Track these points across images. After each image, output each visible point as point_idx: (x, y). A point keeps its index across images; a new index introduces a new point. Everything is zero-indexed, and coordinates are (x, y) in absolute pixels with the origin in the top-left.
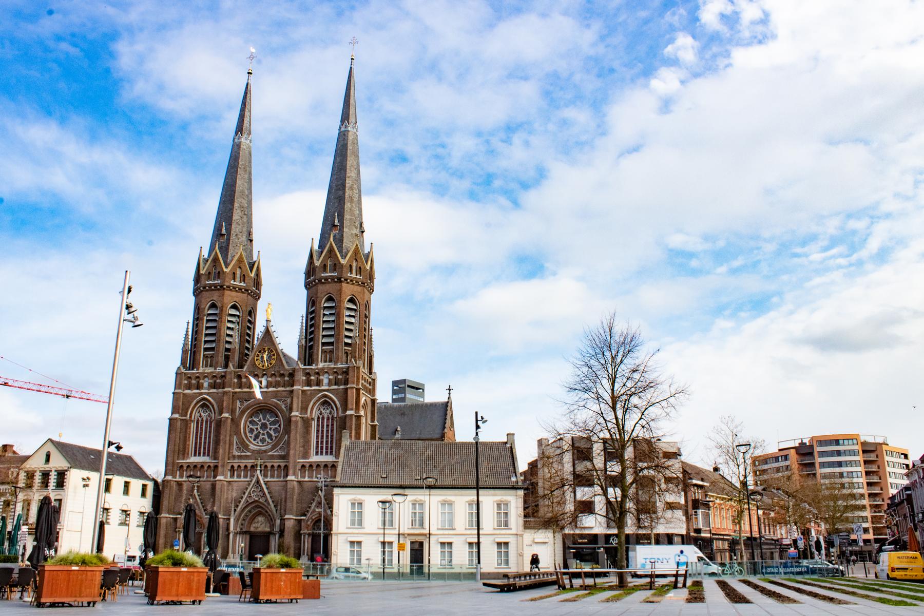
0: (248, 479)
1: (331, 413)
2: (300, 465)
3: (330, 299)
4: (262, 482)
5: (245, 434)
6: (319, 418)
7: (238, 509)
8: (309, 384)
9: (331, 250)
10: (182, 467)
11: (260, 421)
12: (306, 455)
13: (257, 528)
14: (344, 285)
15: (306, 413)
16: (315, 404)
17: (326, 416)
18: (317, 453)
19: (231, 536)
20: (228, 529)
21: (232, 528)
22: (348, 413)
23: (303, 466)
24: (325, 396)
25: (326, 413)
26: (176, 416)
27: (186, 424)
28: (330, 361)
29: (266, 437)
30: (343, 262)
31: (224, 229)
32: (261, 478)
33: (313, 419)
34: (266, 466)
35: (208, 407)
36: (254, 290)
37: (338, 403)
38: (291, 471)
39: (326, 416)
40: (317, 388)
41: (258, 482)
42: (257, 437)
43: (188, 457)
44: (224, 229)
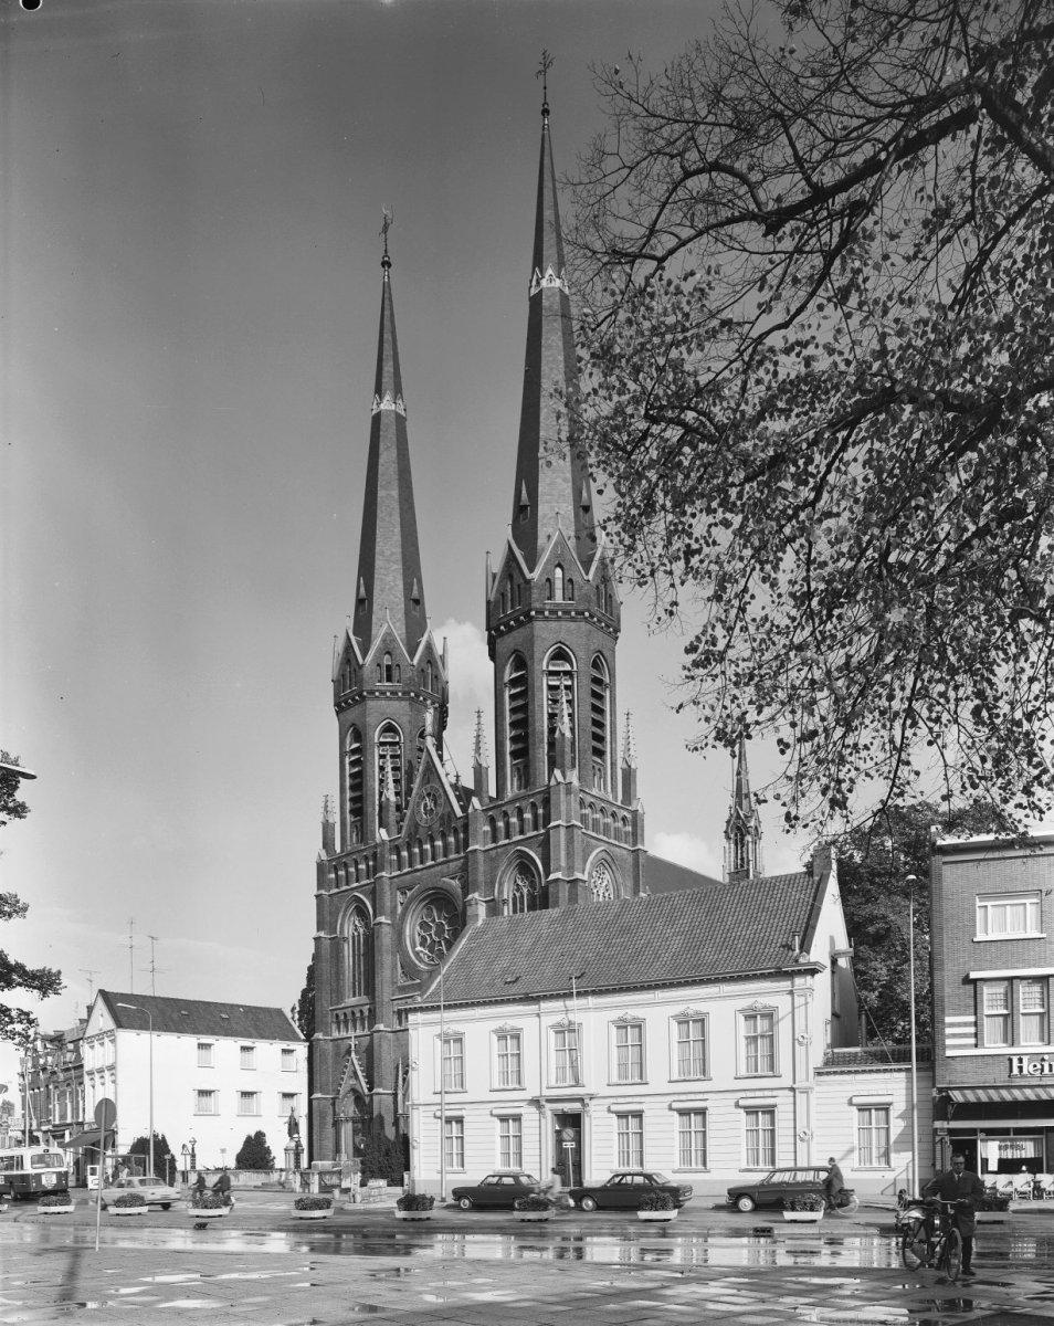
5: (414, 946)
6: (515, 898)
14: (538, 625)
22: (552, 877)
26: (322, 934)
27: (337, 943)
30: (535, 575)
33: (505, 902)
39: (525, 890)
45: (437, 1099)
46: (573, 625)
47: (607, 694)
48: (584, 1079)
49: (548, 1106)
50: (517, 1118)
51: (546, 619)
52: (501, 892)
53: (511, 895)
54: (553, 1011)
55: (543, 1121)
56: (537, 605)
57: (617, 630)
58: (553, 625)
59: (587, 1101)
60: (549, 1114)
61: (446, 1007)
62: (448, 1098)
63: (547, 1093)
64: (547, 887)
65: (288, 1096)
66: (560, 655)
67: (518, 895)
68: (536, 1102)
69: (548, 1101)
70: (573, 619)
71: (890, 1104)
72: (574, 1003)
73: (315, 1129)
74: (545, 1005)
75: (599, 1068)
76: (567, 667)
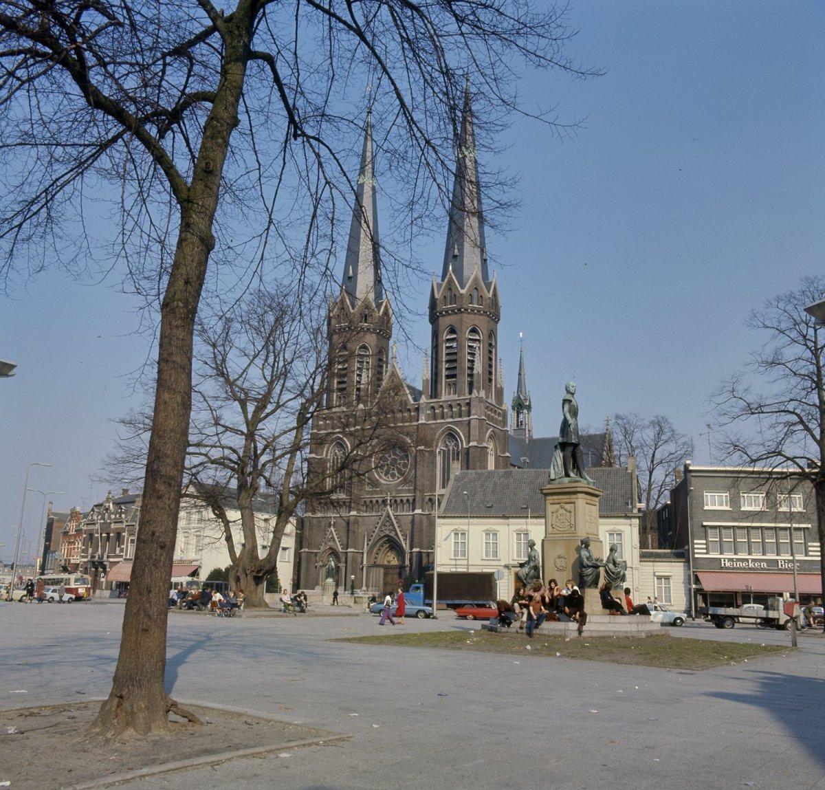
0: (379, 514)
2: (428, 498)
3: (453, 331)
4: (393, 518)
7: (370, 543)
8: (435, 418)
9: (451, 278)
11: (390, 456)
12: (433, 488)
13: (389, 562)
17: (451, 448)
19: (365, 569)
20: (362, 562)
21: (365, 563)
24: (451, 429)
25: (451, 445)
28: (455, 393)
31: (351, 271)
32: (391, 513)
34: (396, 501)
36: (384, 331)
37: (461, 434)
38: (418, 505)
39: (451, 448)
40: (442, 421)
41: (389, 516)
44: (351, 271)
45: (454, 562)
46: (481, 318)
47: (494, 350)
49: (513, 569)
51: (469, 313)
56: (465, 306)
57: (499, 320)
58: (471, 316)
60: (513, 573)
61: (471, 517)
62: (459, 562)
64: (468, 449)
66: (474, 331)
68: (507, 567)
69: (513, 567)
70: (482, 315)
72: (529, 520)
73: (303, 566)
74: (511, 520)
76: (478, 338)
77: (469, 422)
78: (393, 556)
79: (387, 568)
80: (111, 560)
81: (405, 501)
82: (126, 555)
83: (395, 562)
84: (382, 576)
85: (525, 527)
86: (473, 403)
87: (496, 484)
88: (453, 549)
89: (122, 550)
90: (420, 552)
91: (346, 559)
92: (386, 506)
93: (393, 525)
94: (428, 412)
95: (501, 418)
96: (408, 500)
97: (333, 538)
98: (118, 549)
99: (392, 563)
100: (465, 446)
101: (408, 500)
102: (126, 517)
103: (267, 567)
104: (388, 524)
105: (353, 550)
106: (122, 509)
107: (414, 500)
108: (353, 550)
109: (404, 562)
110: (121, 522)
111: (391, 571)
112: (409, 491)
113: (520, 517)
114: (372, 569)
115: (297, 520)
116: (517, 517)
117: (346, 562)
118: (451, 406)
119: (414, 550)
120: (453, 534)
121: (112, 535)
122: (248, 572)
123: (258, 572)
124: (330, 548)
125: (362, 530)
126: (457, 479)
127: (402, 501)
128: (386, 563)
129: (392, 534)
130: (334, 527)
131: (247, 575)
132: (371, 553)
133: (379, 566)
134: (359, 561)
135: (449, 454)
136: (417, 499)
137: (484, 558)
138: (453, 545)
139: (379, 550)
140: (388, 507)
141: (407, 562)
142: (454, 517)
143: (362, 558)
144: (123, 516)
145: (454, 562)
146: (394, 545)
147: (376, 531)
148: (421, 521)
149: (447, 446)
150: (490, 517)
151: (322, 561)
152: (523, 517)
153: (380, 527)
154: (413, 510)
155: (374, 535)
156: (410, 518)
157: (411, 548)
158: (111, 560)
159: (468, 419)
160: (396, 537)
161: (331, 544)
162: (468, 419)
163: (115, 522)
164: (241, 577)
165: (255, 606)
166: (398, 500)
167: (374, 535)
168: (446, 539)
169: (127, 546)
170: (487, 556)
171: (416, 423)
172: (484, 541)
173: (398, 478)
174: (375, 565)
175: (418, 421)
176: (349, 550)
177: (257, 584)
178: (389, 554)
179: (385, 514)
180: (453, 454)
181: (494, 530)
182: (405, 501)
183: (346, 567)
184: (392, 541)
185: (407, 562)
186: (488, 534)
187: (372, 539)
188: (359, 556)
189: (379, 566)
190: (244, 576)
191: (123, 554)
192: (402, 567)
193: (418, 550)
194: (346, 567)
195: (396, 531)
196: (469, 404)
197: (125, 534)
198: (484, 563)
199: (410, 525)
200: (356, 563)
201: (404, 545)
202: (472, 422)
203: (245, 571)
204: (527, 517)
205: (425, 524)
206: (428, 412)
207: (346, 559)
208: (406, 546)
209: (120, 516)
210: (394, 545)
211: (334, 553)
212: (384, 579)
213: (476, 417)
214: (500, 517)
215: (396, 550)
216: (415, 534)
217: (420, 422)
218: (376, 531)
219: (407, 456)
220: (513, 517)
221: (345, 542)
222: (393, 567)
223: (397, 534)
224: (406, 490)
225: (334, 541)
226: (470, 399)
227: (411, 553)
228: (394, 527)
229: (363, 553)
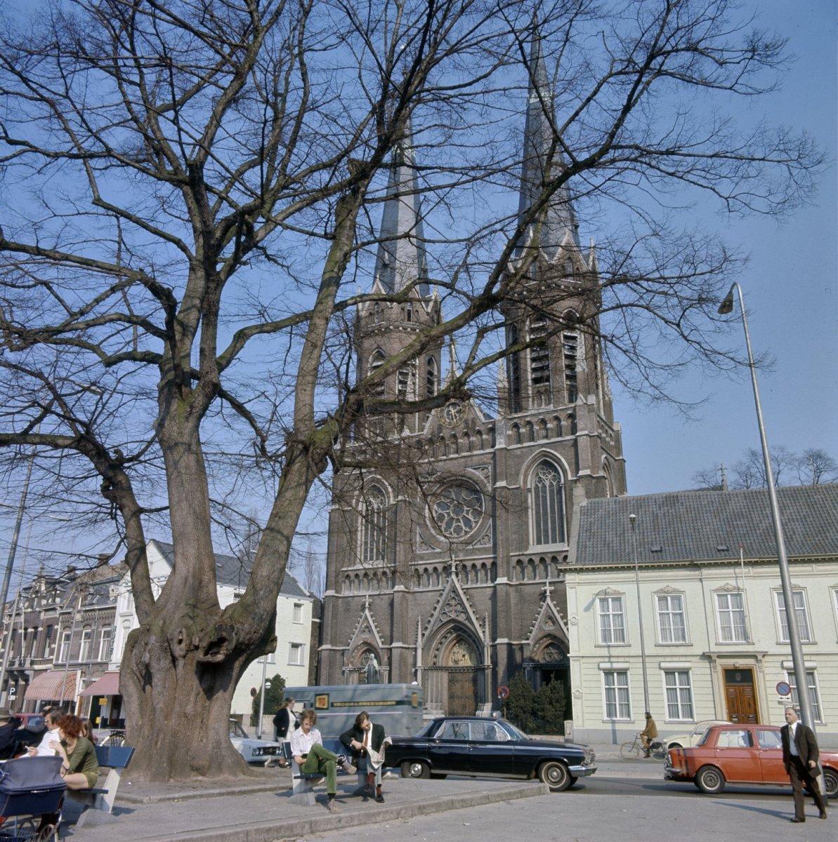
0: (440, 587)
1: (554, 478)
2: (515, 559)
4: (461, 592)
6: (537, 487)
7: (427, 633)
8: (520, 441)
10: (348, 576)
12: (524, 543)
13: (456, 662)
15: (517, 481)
16: (529, 467)
17: (547, 483)
18: (539, 542)
19: (419, 674)
20: (415, 664)
21: (419, 664)
23: (519, 562)
24: (546, 454)
25: (548, 479)
29: (462, 524)
32: (458, 586)
33: (529, 490)
34: (464, 567)
35: (380, 491)
38: (500, 571)
39: (547, 483)
41: (454, 590)
42: (449, 525)
43: (355, 564)
45: (604, 652)
48: (755, 635)
49: (719, 661)
50: (685, 672)
52: (525, 482)
53: (533, 485)
54: (719, 578)
55: (715, 675)
59: (760, 657)
61: (641, 568)
62: (614, 652)
63: (714, 649)
65: (295, 646)
67: (540, 485)
68: (707, 657)
69: (719, 657)
71: (627, 669)
72: (743, 570)
74: (705, 572)
75: (766, 633)
77: (576, 441)
78: (462, 652)
79: (452, 672)
80: (36, 667)
81: (479, 566)
82: (57, 659)
83: (467, 662)
84: (446, 685)
85: (732, 583)
86: (579, 413)
87: (655, 517)
88: (599, 628)
89: (52, 653)
90: (509, 645)
91: (390, 659)
92: (449, 574)
93: (462, 604)
94: (509, 432)
95: (612, 443)
96: (484, 565)
97: (368, 627)
98: (47, 650)
99: (461, 664)
100: (570, 478)
101: (484, 565)
102: (61, 602)
103: (246, 629)
104: (453, 602)
105: (400, 644)
106: (56, 590)
107: (494, 564)
108: (400, 644)
109: (481, 660)
110: (54, 609)
111: (459, 677)
112: (485, 550)
113: (723, 565)
114: (430, 673)
115: (314, 603)
116: (716, 565)
117: (390, 664)
118: (544, 422)
119: (499, 641)
120: (597, 601)
121: (40, 629)
122: (179, 650)
123: (214, 646)
124: (365, 643)
125: (414, 613)
126: (585, 512)
127: (474, 566)
128: (451, 664)
129: (462, 618)
130: (370, 610)
131: (174, 660)
132: (429, 649)
133: (441, 669)
134: (410, 660)
135: (544, 492)
136: (499, 562)
137: (660, 642)
138: (599, 619)
139: (441, 643)
140: (454, 576)
141: (488, 661)
142: (599, 570)
143: (415, 657)
144: (58, 600)
145: (604, 652)
146: (464, 635)
147: (436, 613)
148: (507, 594)
149: (540, 480)
150: (665, 567)
151: (352, 663)
152: (729, 565)
153: (442, 608)
154: (493, 580)
155: (432, 620)
156: (489, 591)
157: (494, 639)
158: (36, 667)
159: (573, 437)
160: (467, 623)
161: (366, 636)
162: (573, 437)
163: (46, 610)
164: (155, 668)
165: (199, 770)
166: (469, 564)
167: (432, 620)
168: (587, 609)
169: (60, 645)
170: (664, 638)
171: (492, 450)
172: (658, 611)
173: (466, 532)
174: (435, 668)
175: (493, 446)
176: (394, 645)
177: (210, 692)
178: (455, 649)
179: (448, 587)
180: (551, 491)
181: (675, 591)
182: (479, 566)
183: (390, 671)
184: (460, 629)
185: (488, 661)
186: (663, 599)
187: (429, 627)
188: (410, 654)
189: (441, 669)
190: (166, 663)
191: (54, 657)
192: (479, 670)
193: (506, 640)
194: (390, 671)
195: (466, 612)
196: (572, 416)
197: (58, 627)
198: (666, 651)
199: (490, 602)
200: (406, 665)
201: (481, 635)
202: (580, 440)
203: (167, 646)
204: (738, 564)
205: (513, 601)
206: (509, 432)
207: (390, 659)
208: (484, 635)
209: (54, 601)
210: (464, 635)
211: (370, 648)
212: (450, 688)
213: (586, 432)
214: (684, 567)
215: (466, 642)
216: (499, 615)
217: (497, 447)
218: (436, 613)
219: (479, 500)
220: (710, 566)
221: (388, 633)
222: (464, 670)
223: (469, 619)
224: (479, 549)
225: (370, 631)
226: (574, 409)
227: (494, 647)
228: (464, 608)
229: (415, 649)
